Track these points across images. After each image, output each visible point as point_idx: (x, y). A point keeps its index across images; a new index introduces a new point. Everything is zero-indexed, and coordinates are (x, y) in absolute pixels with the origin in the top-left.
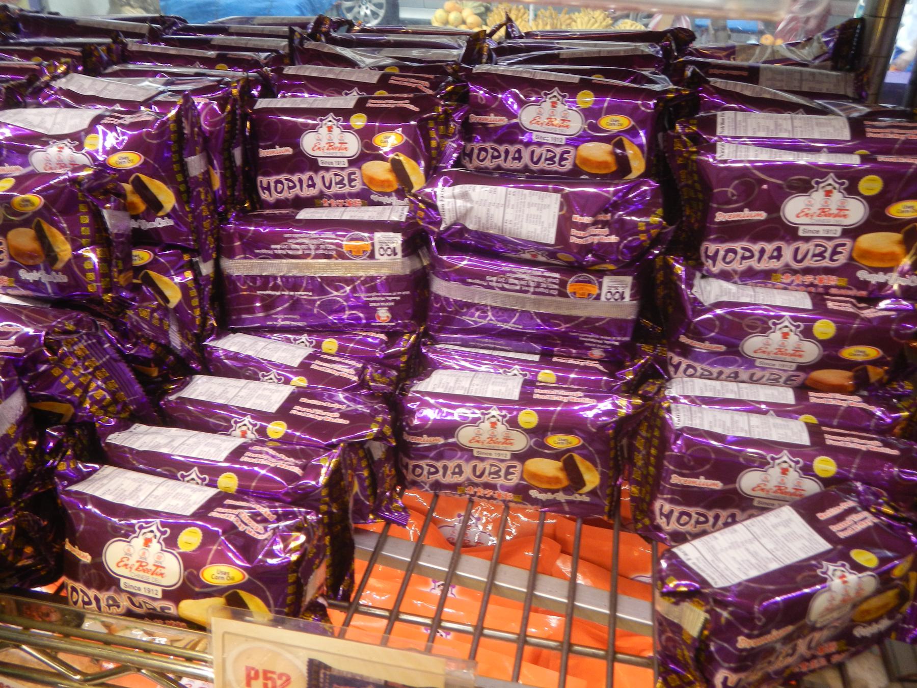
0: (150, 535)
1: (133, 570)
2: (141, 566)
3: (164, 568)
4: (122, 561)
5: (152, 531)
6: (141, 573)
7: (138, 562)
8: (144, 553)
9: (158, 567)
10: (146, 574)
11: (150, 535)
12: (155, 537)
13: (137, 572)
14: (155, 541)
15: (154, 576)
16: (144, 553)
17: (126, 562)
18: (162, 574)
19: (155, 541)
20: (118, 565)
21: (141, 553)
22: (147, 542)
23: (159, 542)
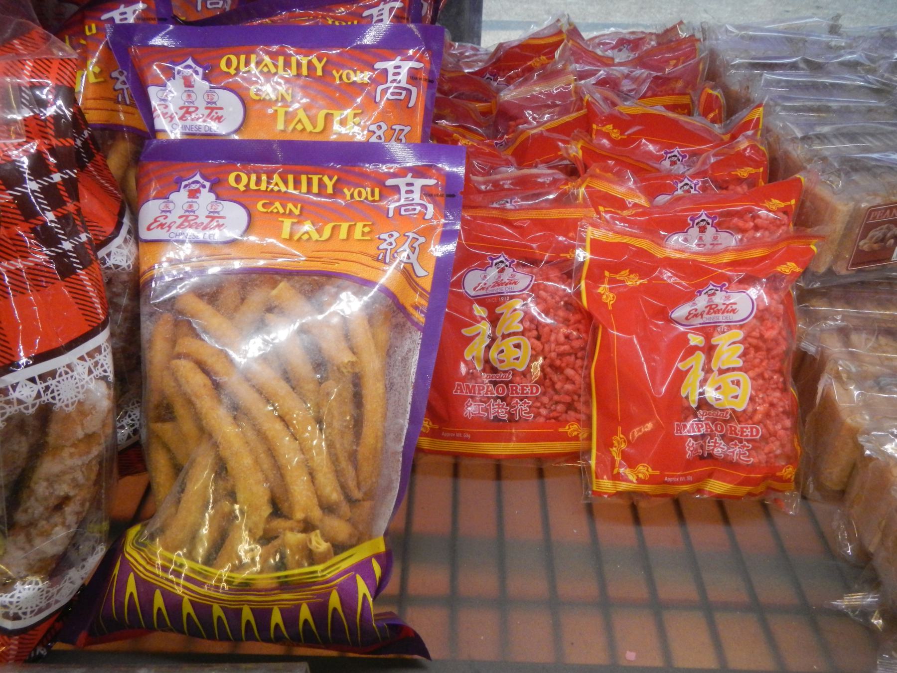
4: (156, 221)
7: (180, 217)
8: (191, 206)
12: (204, 187)
16: (191, 206)
17: (164, 221)
21: (186, 207)
22: (193, 194)
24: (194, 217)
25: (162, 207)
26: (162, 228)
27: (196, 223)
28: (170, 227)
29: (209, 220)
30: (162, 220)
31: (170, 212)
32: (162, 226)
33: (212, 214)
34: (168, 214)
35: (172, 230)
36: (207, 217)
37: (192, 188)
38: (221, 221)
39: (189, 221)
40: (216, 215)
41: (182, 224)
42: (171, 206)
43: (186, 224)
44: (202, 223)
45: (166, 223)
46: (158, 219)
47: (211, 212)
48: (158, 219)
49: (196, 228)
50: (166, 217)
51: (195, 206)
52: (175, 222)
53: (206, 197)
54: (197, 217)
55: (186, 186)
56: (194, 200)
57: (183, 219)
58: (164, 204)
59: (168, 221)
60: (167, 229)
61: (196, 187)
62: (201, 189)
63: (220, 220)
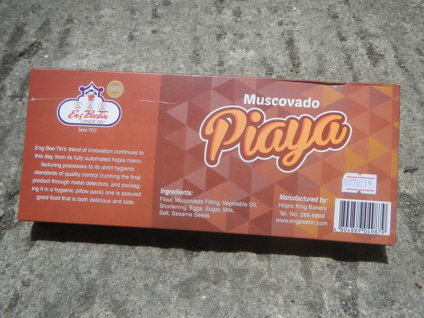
0: (91, 93)
1: (82, 118)
2: (89, 113)
3: (107, 112)
4: (73, 113)
5: (92, 91)
6: (89, 119)
7: (86, 111)
8: (90, 105)
9: (102, 112)
10: (93, 119)
11: (91, 93)
12: (96, 94)
13: (85, 119)
14: (96, 96)
15: (99, 119)
16: (90, 105)
17: (77, 114)
18: (105, 117)
19: (96, 96)
20: (69, 117)
21: (88, 105)
22: (91, 98)
23: (99, 96)
24: (92, 112)
25: (75, 105)
26: (77, 117)
27: (94, 115)
28: (81, 117)
29: (100, 113)
30: (76, 112)
31: (80, 108)
32: (76, 116)
33: (101, 110)
34: (79, 109)
35: (81, 119)
36: (99, 111)
37: (89, 94)
38: (106, 114)
39: (90, 114)
40: (103, 110)
41: (86, 115)
42: (80, 105)
43: (89, 115)
44: (97, 115)
45: (78, 115)
46: (74, 112)
47: (101, 109)
48: (74, 112)
49: (94, 118)
50: (78, 111)
51: (93, 105)
52: (83, 114)
53: (98, 100)
54: (94, 111)
55: (86, 93)
56: (92, 102)
57: (87, 112)
58: (76, 104)
59: (80, 113)
60: (79, 118)
61: (92, 94)
62: (94, 95)
63: (105, 113)
